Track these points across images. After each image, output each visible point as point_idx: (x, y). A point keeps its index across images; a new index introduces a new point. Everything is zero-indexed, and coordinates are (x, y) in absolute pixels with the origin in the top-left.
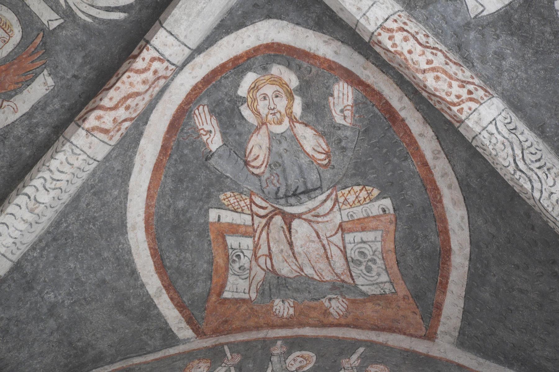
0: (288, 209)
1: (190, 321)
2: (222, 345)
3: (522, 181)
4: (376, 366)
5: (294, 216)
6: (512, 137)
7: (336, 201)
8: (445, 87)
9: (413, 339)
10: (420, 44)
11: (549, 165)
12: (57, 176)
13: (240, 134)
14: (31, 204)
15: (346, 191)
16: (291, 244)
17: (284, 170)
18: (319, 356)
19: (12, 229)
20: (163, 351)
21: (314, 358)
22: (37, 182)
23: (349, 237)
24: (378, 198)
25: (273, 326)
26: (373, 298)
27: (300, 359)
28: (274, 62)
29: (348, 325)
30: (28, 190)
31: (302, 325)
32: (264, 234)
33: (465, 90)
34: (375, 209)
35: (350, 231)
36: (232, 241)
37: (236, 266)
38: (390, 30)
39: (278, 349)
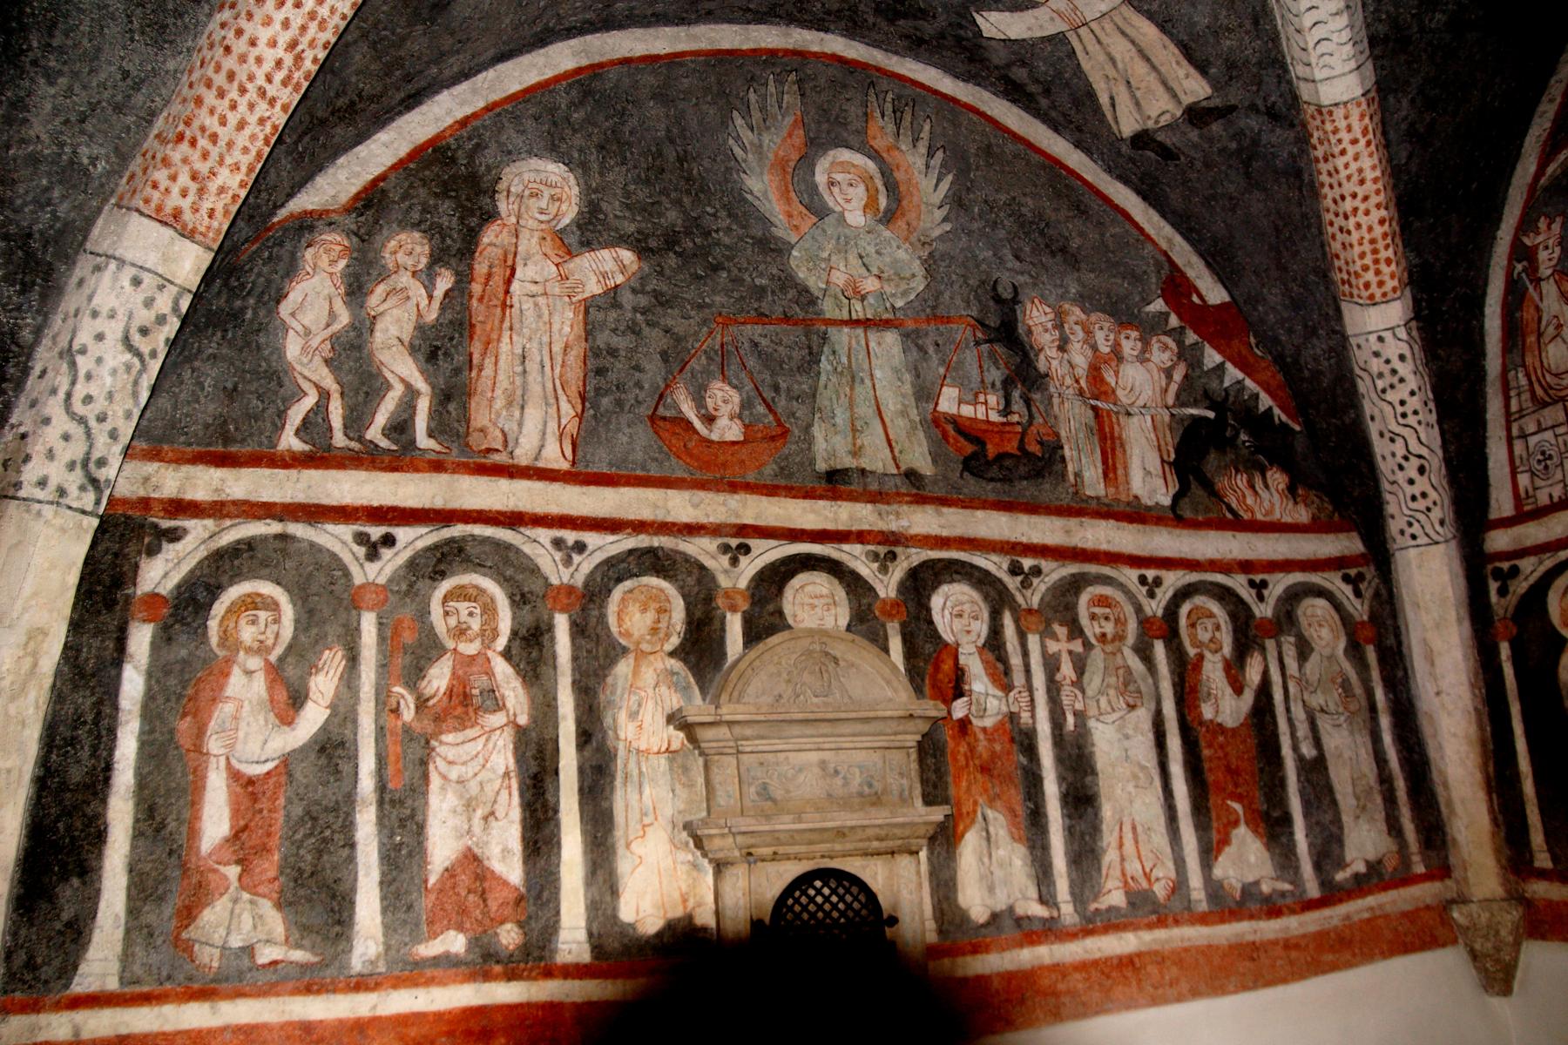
19: (1335, 37)
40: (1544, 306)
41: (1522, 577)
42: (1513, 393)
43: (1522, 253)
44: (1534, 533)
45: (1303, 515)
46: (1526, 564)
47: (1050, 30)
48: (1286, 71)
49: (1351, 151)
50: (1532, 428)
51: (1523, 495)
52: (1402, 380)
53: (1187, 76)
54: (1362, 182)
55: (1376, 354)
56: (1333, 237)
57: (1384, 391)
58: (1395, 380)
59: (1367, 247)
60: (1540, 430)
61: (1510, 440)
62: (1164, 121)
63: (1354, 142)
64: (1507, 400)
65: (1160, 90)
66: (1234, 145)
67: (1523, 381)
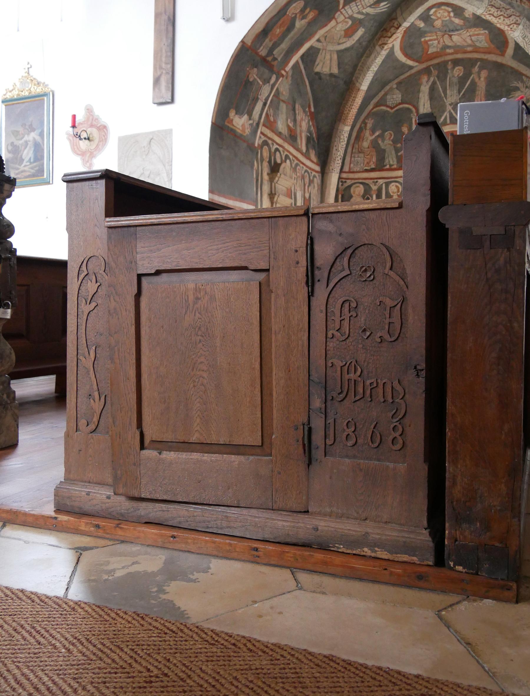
0: (450, 33)
1: (417, 61)
2: (430, 66)
5: (452, 35)
6: (524, 41)
10: (495, 17)
12: (378, 63)
16: (452, 40)
18: (464, 68)
20: (410, 71)
21: (463, 70)
22: (373, 67)
26: (483, 48)
27: (458, 71)
30: (371, 69)
31: (457, 53)
32: (442, 39)
37: (432, 46)
39: (450, 66)
40: (366, 134)
41: (347, 183)
43: (364, 123)
44: (351, 176)
45: (315, 160)
46: (348, 181)
47: (319, 47)
48: (353, 77)
50: (357, 156)
55: (343, 135)
56: (346, 110)
59: (351, 115)
60: (358, 157)
64: (352, 150)
65: (328, 67)
66: (334, 84)
67: (357, 147)
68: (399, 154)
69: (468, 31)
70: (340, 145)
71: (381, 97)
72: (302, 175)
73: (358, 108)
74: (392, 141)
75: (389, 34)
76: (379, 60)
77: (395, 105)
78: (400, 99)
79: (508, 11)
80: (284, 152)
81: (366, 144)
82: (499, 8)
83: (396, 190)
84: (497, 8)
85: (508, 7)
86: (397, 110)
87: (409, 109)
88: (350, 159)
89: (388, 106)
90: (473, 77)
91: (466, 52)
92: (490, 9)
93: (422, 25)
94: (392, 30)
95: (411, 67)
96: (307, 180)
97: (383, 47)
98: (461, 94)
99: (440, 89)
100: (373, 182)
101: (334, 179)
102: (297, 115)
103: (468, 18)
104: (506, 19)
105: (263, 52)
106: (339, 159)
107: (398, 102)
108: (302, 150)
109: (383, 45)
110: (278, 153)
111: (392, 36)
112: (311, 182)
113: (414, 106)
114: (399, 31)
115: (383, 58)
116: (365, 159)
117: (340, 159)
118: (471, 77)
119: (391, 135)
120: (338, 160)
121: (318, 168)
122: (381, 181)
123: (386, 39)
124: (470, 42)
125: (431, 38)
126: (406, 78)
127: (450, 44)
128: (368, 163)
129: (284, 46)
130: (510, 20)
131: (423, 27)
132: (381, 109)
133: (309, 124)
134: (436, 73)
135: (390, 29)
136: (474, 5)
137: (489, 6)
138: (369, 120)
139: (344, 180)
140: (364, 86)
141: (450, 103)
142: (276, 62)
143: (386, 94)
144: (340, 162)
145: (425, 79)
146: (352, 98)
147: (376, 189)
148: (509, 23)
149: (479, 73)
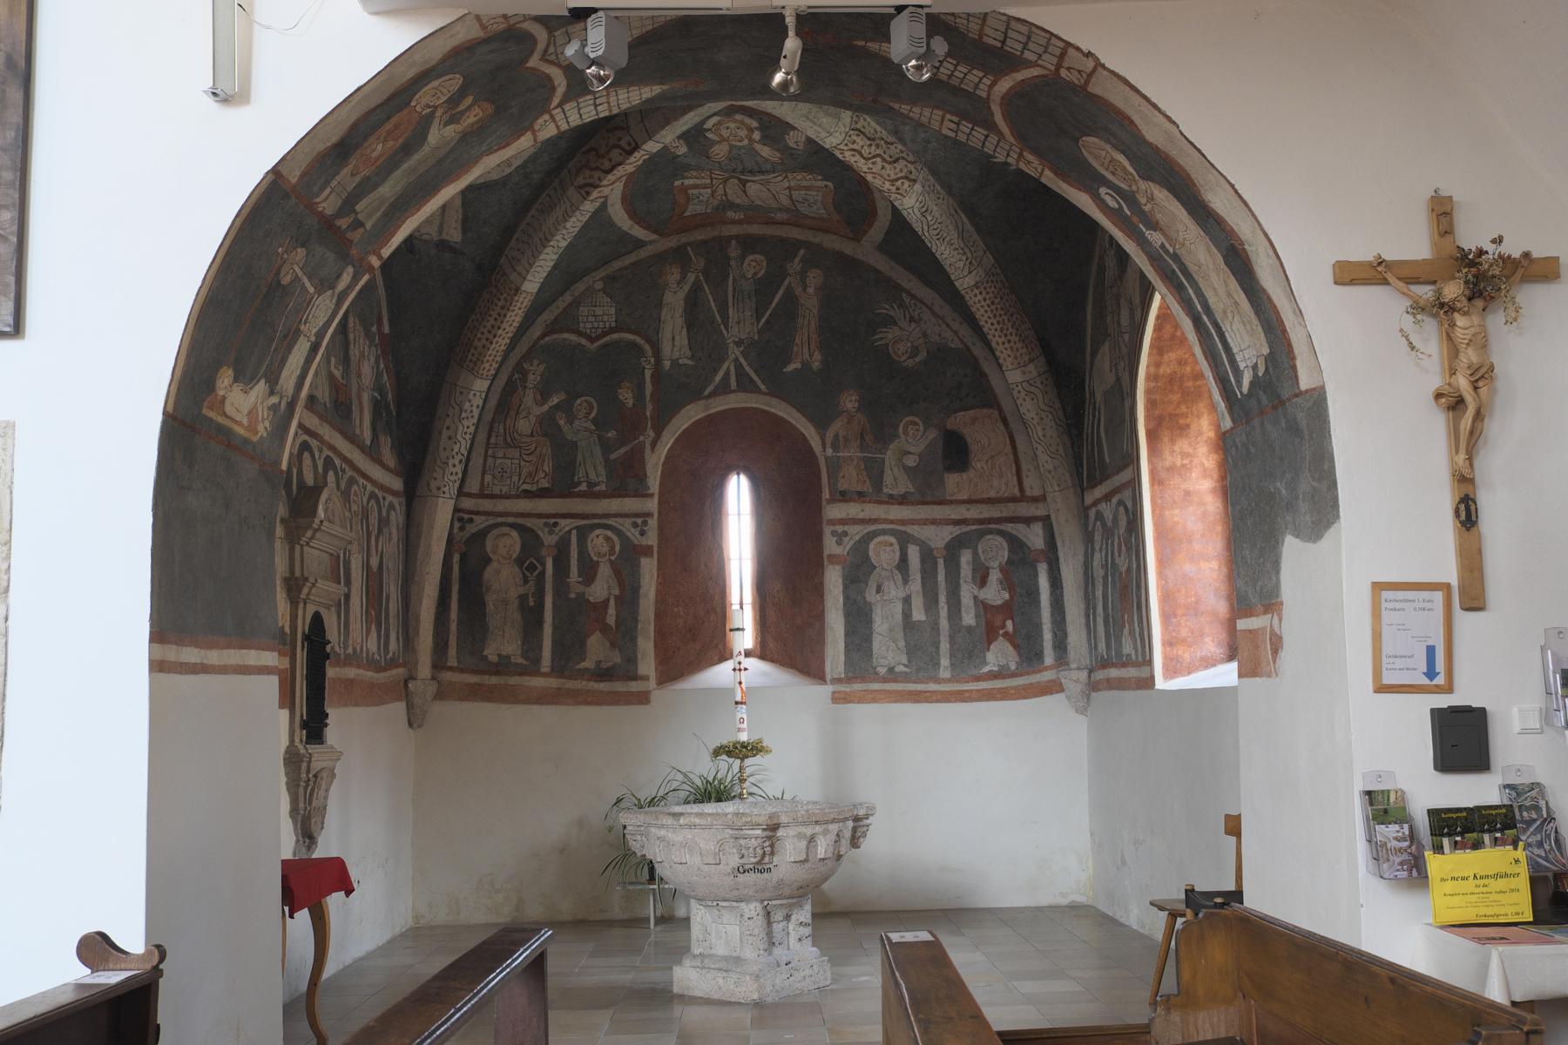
3: (926, 241)
4: (813, 270)
5: (749, 181)
7: (786, 177)
8: (880, 183)
9: (843, 239)
10: (864, 158)
11: (945, 235)
12: (572, 230)
13: (704, 145)
14: (555, 250)
15: (795, 174)
16: (745, 192)
17: (742, 161)
21: (765, 263)
22: (558, 237)
23: (793, 192)
24: (821, 180)
25: (725, 223)
27: (754, 264)
28: (736, 112)
29: (790, 224)
30: (551, 243)
32: (721, 186)
33: (894, 188)
34: (819, 184)
35: (796, 190)
36: (690, 192)
38: (840, 150)
39: (734, 251)
42: (493, 434)
44: (486, 505)
45: (391, 461)
49: (517, 311)
50: (501, 455)
51: (486, 483)
52: (472, 417)
53: (455, 228)
54: (511, 325)
55: (470, 401)
56: (480, 339)
57: (463, 419)
58: (470, 415)
61: (485, 460)
62: (425, 237)
63: (520, 309)
66: (449, 267)
67: (502, 431)
68: (613, 456)
69: (786, 177)
70: (461, 428)
71: (564, 309)
72: (363, 507)
73: (510, 335)
74: (594, 421)
75: (607, 165)
76: (574, 224)
77: (600, 330)
78: (614, 319)
79: (892, 147)
80: (321, 451)
81: (524, 426)
82: (874, 140)
83: (605, 549)
84: (869, 139)
85: (890, 139)
86: (606, 345)
87: (634, 345)
88: (481, 461)
89: (580, 334)
90: (790, 282)
91: (771, 222)
92: (855, 138)
93: (682, 150)
94: (615, 154)
95: (639, 244)
96: (374, 521)
97: (588, 193)
98: (763, 320)
99: (712, 304)
100: (546, 524)
101: (442, 514)
102: (352, 345)
103: (792, 149)
104: (886, 165)
105: (328, 203)
106: (457, 463)
107: (607, 325)
108: (363, 442)
109: (587, 189)
110: (306, 455)
111: (613, 168)
112: (384, 522)
113: (648, 340)
114: (632, 159)
115: (585, 219)
116: (523, 463)
117: (461, 462)
118: (786, 282)
119: (592, 408)
120: (454, 466)
121: (397, 484)
122: (566, 524)
123: (597, 174)
124: (785, 202)
125: (698, 182)
126: (626, 268)
127: (738, 201)
128: (530, 475)
129: (388, 190)
130: (895, 168)
131: (684, 155)
132: (565, 340)
133: (378, 367)
134: (702, 263)
135: (608, 151)
136: (820, 126)
137: (852, 132)
138: (532, 365)
139: (466, 516)
140: (532, 285)
141: (737, 340)
142: (361, 230)
143: (576, 303)
144: (459, 469)
145: (673, 274)
146: (498, 309)
147: (553, 543)
148: (893, 177)
149: (803, 275)
